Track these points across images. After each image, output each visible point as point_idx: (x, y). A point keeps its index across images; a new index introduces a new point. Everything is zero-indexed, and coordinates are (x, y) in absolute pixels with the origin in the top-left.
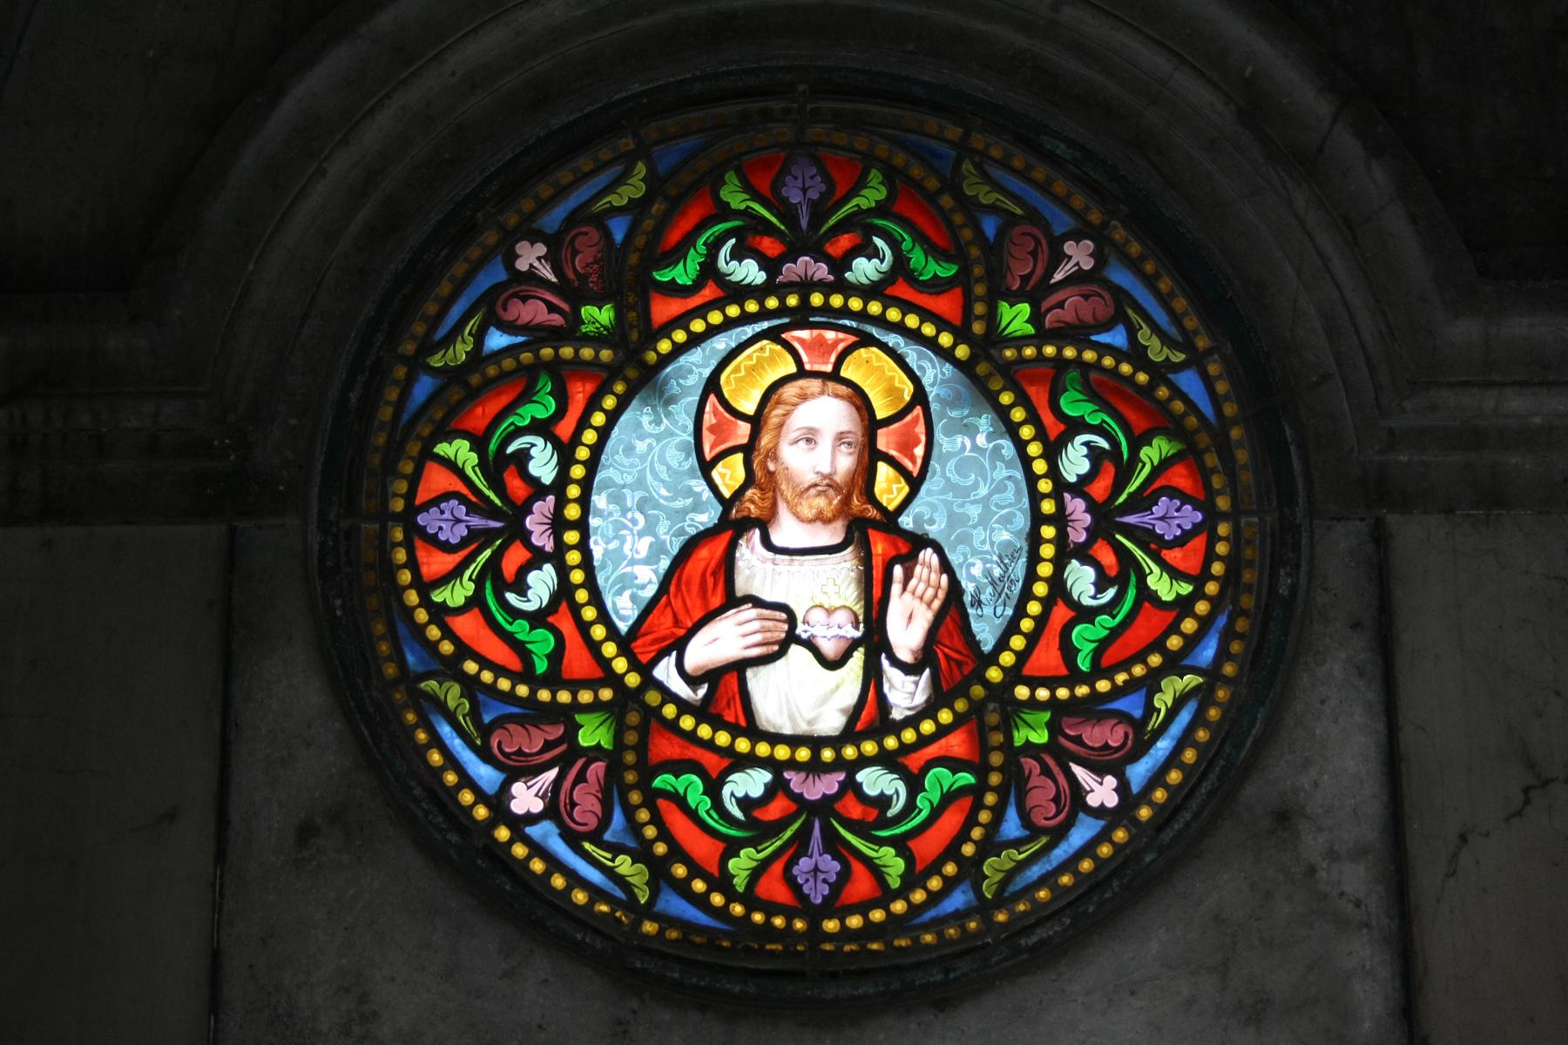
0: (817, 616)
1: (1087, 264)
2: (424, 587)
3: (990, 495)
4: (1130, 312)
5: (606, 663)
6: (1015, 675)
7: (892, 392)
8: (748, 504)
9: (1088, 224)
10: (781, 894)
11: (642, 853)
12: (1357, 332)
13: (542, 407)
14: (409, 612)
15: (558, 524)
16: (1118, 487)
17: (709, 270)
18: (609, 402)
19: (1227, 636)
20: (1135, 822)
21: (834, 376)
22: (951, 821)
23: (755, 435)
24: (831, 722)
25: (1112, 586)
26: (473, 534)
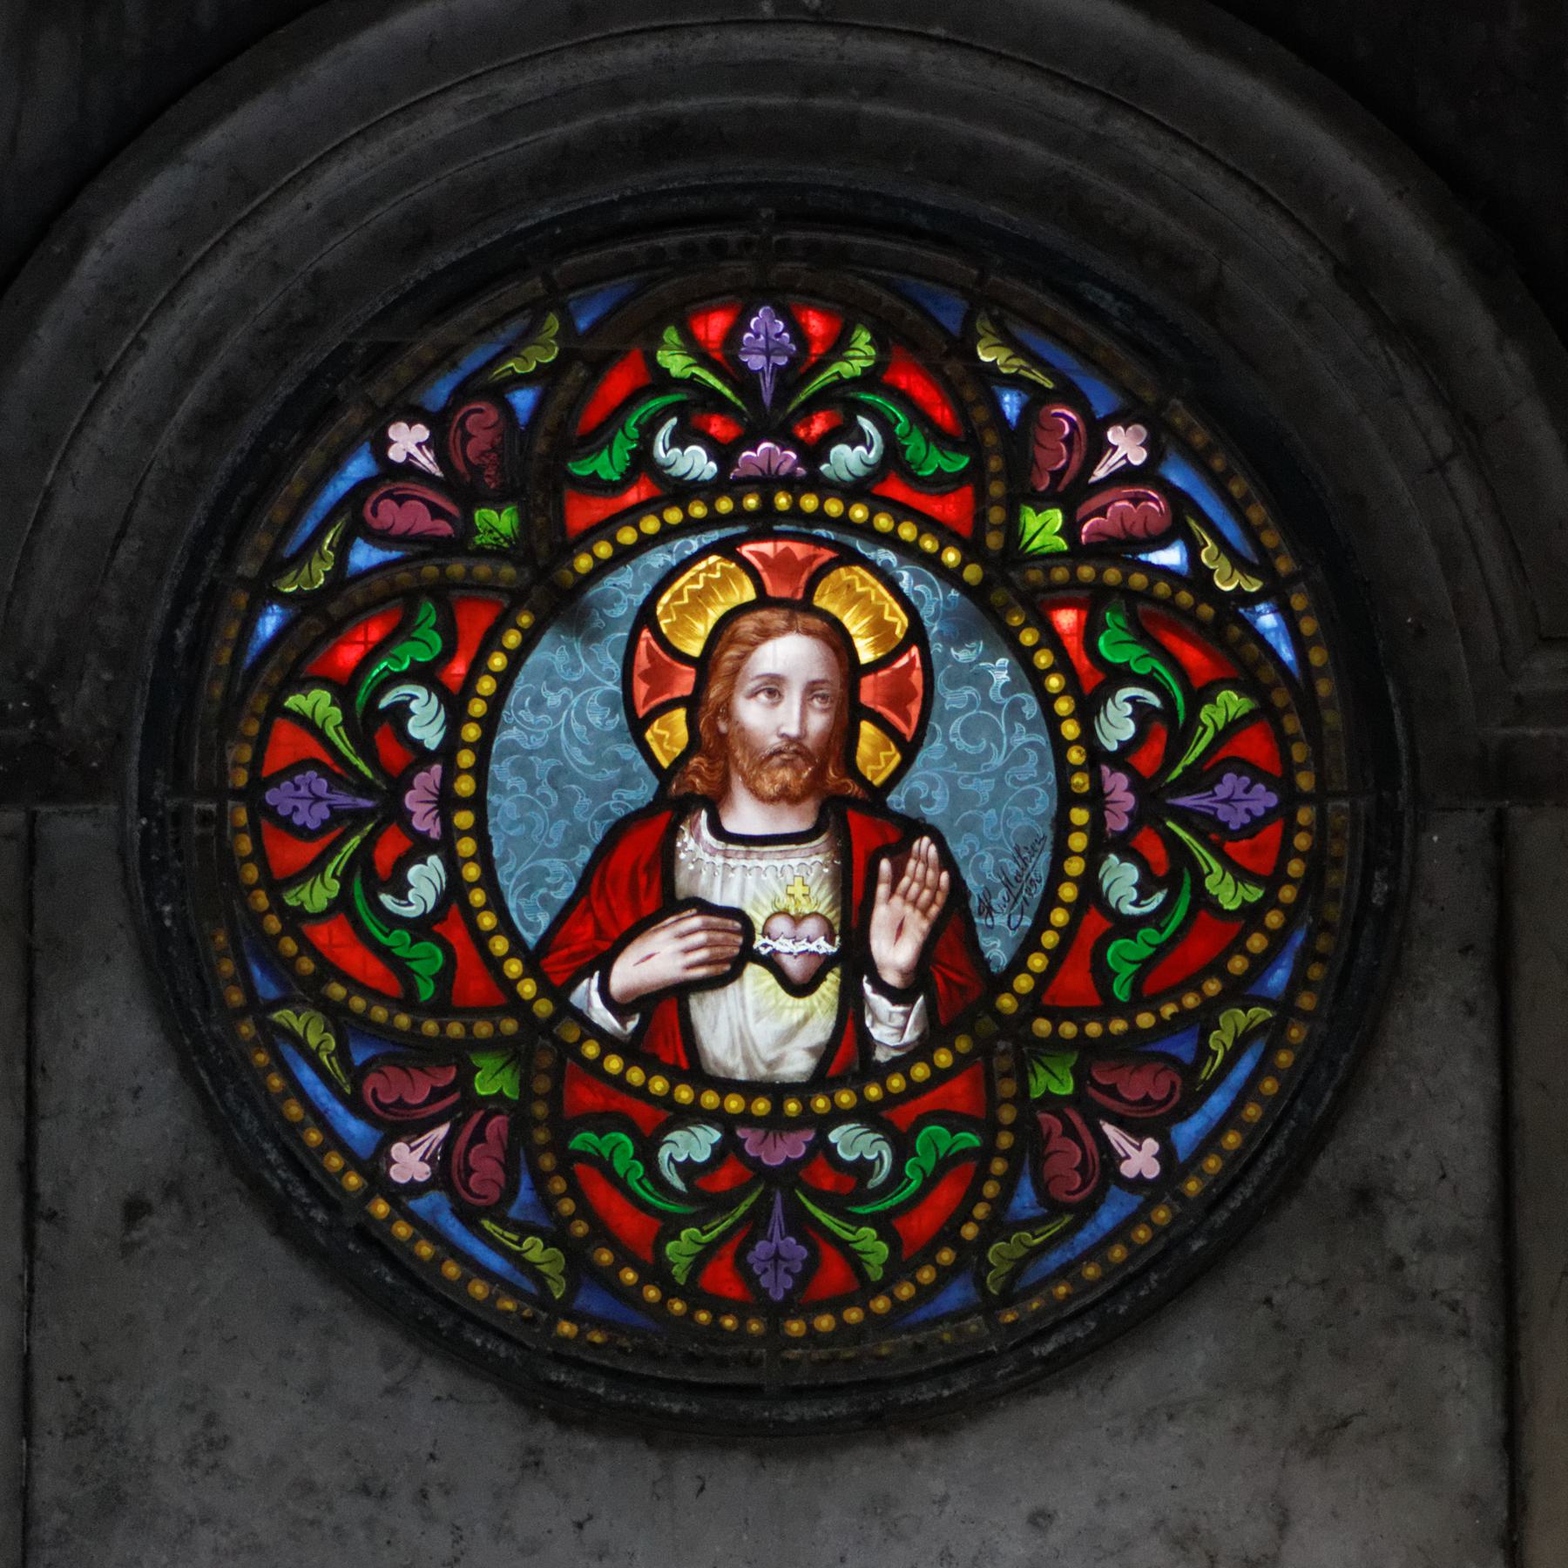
0: (781, 925)
1: (1138, 457)
2: (276, 886)
3: (1006, 766)
4: (1193, 524)
5: (510, 985)
6: (1033, 1005)
7: (880, 628)
8: (691, 777)
9: (1139, 402)
10: (733, 1290)
11: (556, 1237)
12: (1481, 567)
13: (423, 647)
14: (257, 918)
15: (447, 802)
16: (1171, 759)
17: (642, 460)
18: (512, 639)
19: (1308, 955)
20: (1181, 1197)
21: (804, 606)
22: (947, 1195)
23: (701, 685)
24: (797, 1064)
25: (1160, 889)
26: (337, 815)
